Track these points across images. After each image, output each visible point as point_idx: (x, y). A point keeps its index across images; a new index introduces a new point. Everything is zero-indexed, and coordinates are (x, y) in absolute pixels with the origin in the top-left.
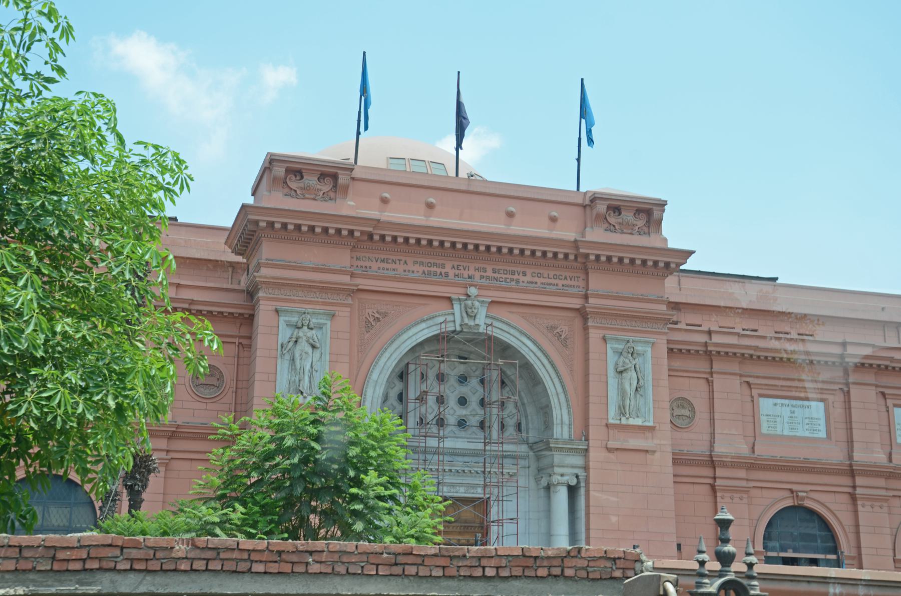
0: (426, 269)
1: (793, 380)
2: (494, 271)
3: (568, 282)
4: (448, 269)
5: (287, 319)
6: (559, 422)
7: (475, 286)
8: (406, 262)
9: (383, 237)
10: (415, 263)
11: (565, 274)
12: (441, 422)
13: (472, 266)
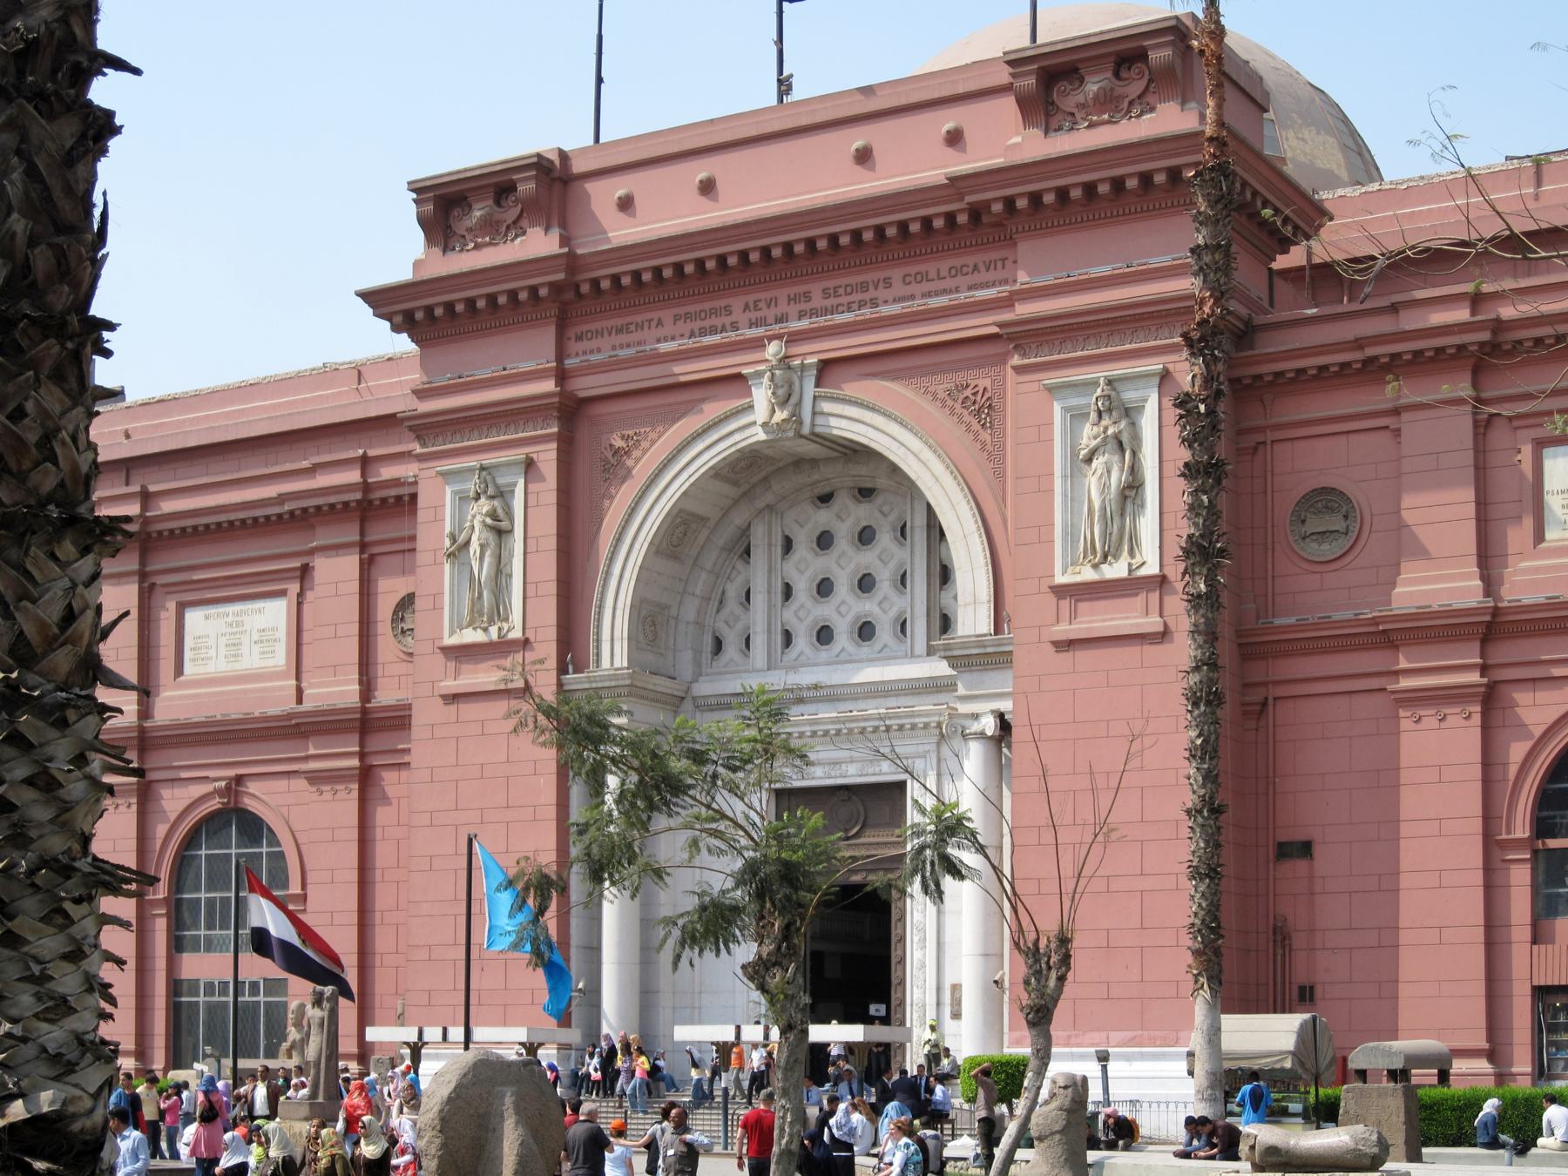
0: (697, 325)
1: (1528, 397)
2: (826, 293)
3: (983, 276)
4: (738, 315)
5: (457, 487)
6: (970, 599)
7: (779, 337)
8: (660, 323)
9: (595, 283)
10: (676, 318)
11: (970, 260)
12: (824, 635)
13: (782, 293)
